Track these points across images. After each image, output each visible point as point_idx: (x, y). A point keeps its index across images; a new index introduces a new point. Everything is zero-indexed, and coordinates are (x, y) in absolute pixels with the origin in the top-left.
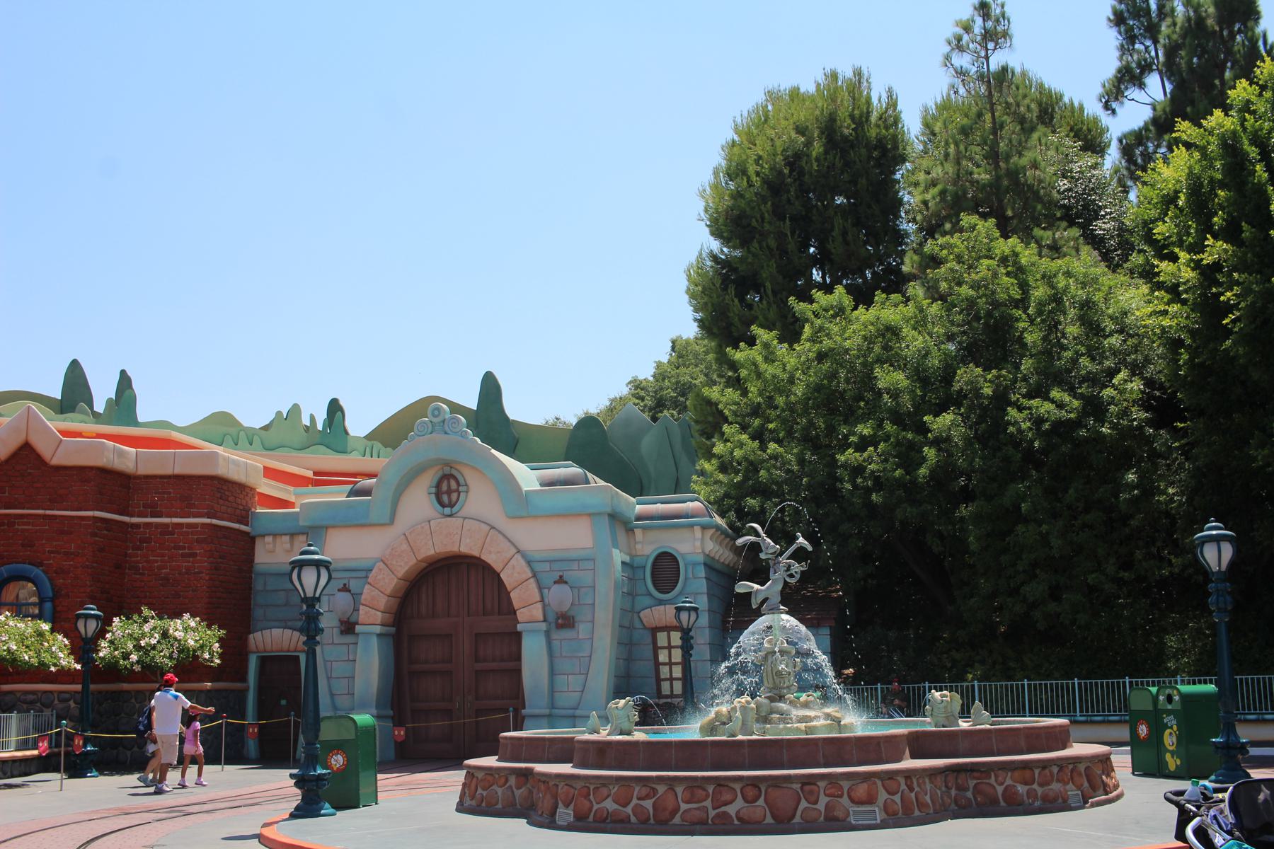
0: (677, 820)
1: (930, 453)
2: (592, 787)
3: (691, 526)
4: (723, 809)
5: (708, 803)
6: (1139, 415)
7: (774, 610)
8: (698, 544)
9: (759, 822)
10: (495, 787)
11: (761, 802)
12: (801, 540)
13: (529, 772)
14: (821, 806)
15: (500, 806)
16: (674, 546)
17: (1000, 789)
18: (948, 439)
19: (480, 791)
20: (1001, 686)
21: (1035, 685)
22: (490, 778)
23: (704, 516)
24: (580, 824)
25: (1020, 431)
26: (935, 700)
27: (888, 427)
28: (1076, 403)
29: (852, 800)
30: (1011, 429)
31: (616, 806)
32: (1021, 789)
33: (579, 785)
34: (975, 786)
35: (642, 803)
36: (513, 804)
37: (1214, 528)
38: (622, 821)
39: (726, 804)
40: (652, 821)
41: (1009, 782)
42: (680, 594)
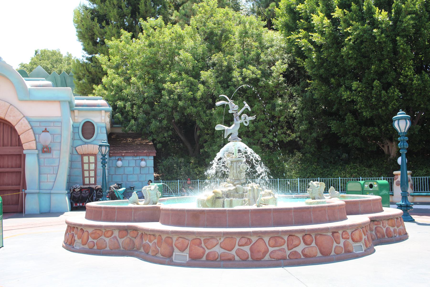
0: (267, 257)
1: (201, 86)
2: (202, 239)
3: (101, 110)
4: (294, 249)
5: (285, 246)
6: (282, 79)
7: (234, 140)
8: (103, 118)
9: (315, 256)
10: (103, 237)
11: (313, 244)
12: (246, 105)
13: (135, 229)
14: (342, 245)
15: (108, 249)
16: (93, 119)
17: (384, 230)
18: (207, 82)
19: (90, 239)
20: (419, 178)
21: (424, 179)
22: (98, 232)
23: (106, 106)
24: (194, 262)
25: (238, 81)
26: (314, 186)
27: (184, 75)
28: (260, 72)
29: (353, 240)
30: (234, 80)
31: (223, 251)
32: (392, 229)
33: (190, 238)
34: (376, 228)
35: (241, 248)
36: (119, 247)
37: (401, 114)
38: (230, 260)
39: (296, 246)
40: (250, 259)
41: (387, 226)
42: (95, 140)
